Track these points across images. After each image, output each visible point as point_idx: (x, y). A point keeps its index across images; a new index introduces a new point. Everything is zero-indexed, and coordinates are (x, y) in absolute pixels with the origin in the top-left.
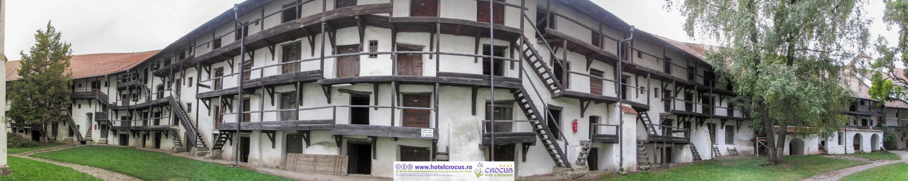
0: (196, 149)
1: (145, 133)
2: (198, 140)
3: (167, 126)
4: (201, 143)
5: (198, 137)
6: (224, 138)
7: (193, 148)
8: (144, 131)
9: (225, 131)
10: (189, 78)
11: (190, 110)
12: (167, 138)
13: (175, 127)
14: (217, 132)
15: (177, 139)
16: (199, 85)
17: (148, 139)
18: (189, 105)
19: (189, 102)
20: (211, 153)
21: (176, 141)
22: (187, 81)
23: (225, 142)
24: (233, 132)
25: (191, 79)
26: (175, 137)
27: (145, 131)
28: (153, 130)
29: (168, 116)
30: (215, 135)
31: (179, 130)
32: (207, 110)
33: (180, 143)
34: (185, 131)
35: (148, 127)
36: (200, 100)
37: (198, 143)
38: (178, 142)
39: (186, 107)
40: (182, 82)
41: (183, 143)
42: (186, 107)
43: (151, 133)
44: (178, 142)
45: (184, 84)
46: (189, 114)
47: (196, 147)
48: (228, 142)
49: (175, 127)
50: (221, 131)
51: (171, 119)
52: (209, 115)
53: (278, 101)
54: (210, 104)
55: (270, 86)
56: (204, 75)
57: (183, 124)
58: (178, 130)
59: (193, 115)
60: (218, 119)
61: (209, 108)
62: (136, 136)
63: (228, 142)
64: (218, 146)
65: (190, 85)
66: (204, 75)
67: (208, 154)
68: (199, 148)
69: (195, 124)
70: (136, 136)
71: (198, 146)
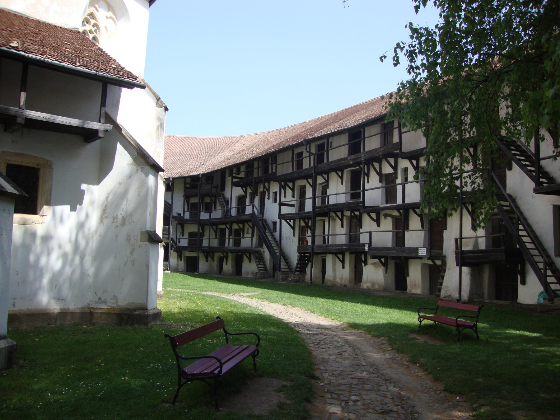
0: (279, 273)
1: (222, 255)
2: (282, 264)
3: (249, 247)
4: (286, 267)
5: (282, 257)
6: (306, 260)
7: (277, 272)
8: (221, 253)
9: (304, 253)
10: (273, 192)
12: (250, 261)
13: (261, 249)
15: (262, 263)
16: (281, 204)
17: (226, 264)
18: (275, 223)
20: (292, 278)
21: (259, 266)
22: (271, 195)
26: (259, 260)
27: (222, 253)
28: (232, 252)
29: (250, 235)
31: (264, 252)
32: (292, 231)
35: (227, 248)
36: (283, 221)
37: (282, 267)
38: (263, 266)
40: (267, 197)
41: (268, 267)
43: (230, 255)
44: (263, 266)
45: (269, 198)
46: (274, 233)
47: (280, 271)
48: (310, 264)
49: (261, 249)
51: (254, 239)
52: (294, 236)
53: (346, 221)
56: (289, 192)
58: (262, 252)
59: (277, 234)
60: (302, 240)
61: (293, 228)
62: (210, 259)
65: (275, 201)
66: (289, 192)
67: (290, 277)
68: (283, 271)
70: (210, 259)
71: (283, 270)
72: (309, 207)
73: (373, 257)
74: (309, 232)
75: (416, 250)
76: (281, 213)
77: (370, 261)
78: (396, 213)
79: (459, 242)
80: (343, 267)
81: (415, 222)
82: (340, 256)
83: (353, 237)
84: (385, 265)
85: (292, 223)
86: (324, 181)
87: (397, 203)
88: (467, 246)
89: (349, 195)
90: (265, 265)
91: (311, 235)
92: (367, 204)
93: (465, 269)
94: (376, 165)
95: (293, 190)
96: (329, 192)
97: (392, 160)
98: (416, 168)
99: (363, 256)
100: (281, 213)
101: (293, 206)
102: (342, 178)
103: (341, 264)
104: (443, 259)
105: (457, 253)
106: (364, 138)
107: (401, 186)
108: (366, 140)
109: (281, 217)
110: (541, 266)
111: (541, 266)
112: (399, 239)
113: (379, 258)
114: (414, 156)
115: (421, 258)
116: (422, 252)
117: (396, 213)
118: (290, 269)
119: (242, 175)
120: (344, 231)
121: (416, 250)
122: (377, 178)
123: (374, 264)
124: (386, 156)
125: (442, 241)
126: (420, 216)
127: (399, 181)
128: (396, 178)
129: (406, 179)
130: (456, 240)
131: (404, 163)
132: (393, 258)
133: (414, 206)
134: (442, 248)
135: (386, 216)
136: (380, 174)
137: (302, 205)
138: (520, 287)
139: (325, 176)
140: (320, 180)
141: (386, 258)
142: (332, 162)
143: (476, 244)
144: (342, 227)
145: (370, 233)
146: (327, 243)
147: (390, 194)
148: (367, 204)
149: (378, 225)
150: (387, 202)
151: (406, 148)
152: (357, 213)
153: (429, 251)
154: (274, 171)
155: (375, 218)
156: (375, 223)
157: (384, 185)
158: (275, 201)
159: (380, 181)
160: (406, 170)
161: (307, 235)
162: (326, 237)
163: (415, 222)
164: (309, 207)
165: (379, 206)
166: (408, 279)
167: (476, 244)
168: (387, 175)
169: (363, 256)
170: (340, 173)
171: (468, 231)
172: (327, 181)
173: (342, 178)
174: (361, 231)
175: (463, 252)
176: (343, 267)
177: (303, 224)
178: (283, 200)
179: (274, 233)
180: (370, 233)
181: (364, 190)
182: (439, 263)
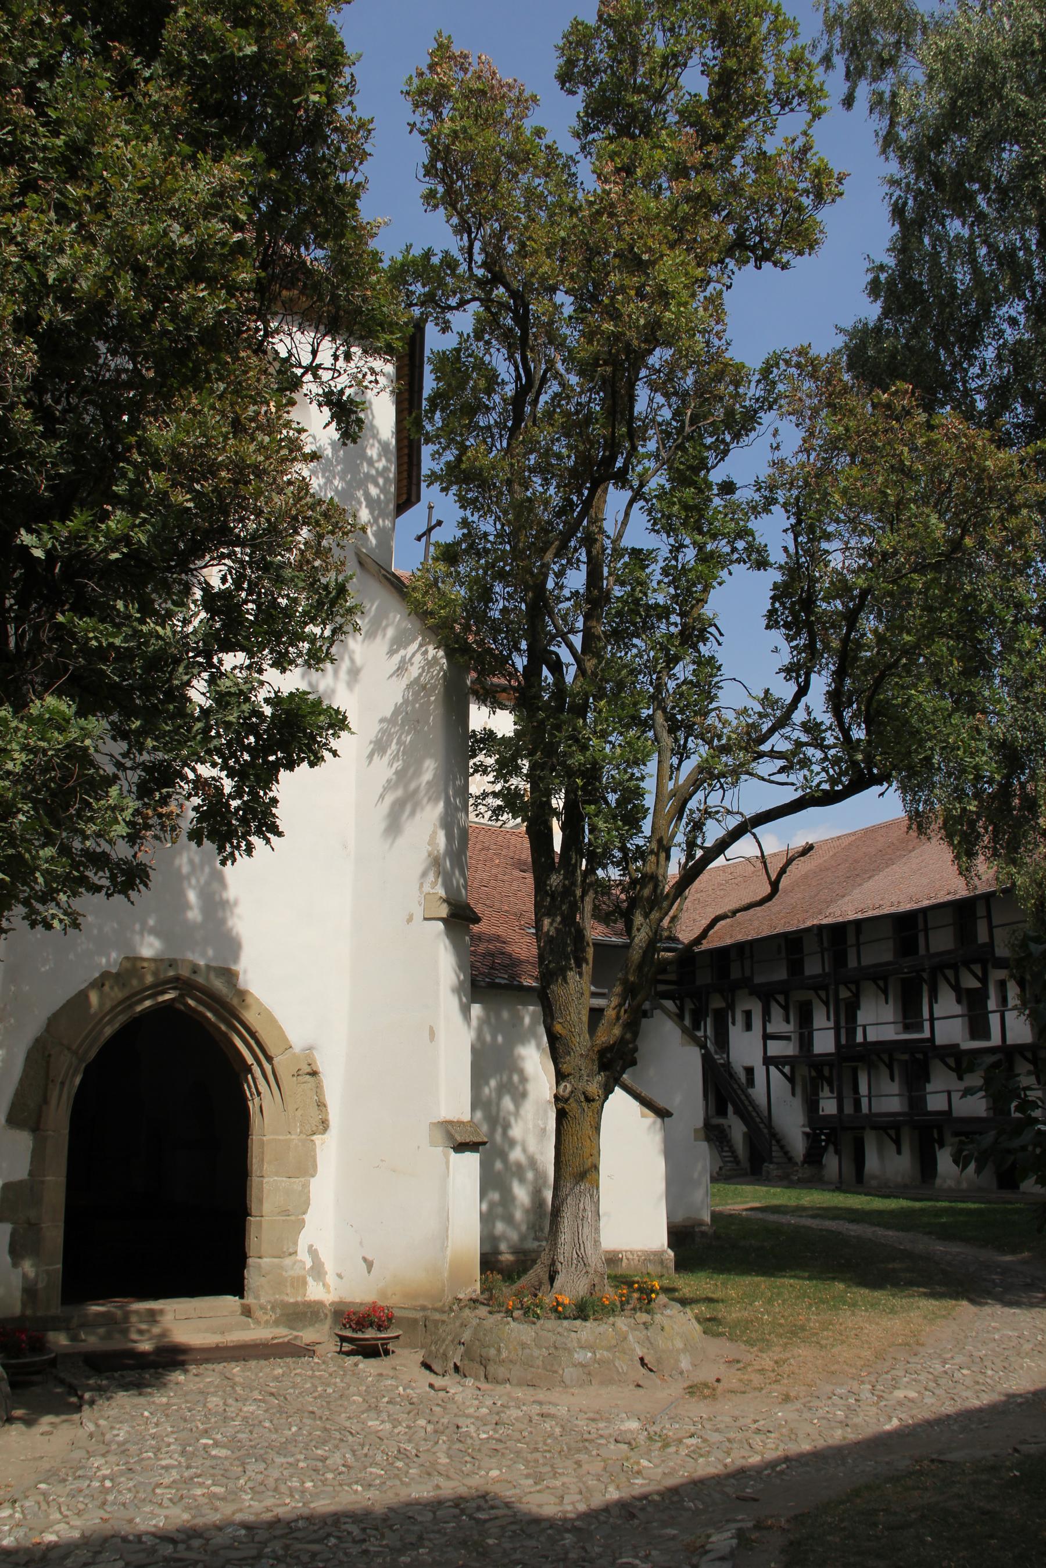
9: (821, 1129)
11: (751, 1082)
14: (808, 1130)
16: (766, 1037)
18: (750, 1071)
19: (748, 1064)
22: (739, 1018)
23: (825, 1148)
25: (748, 1015)
32: (788, 1085)
34: (745, 1129)
36: (772, 1068)
39: (742, 1077)
42: (742, 1077)
45: (734, 1024)
46: (750, 1091)
48: (831, 1149)
52: (793, 1094)
54: (792, 1070)
56: (777, 1012)
57: (738, 1112)
59: (758, 1092)
60: (811, 1106)
61: (791, 1079)
63: (831, 1149)
64: (814, 1156)
65: (748, 1027)
66: (777, 1012)
69: (766, 1113)
72: (824, 1043)
74: (826, 1088)
76: (769, 1054)
80: (899, 1152)
82: (892, 1132)
83: (916, 1101)
85: (787, 1069)
86: (849, 994)
89: (900, 1026)
90: (733, 1151)
91: (830, 1095)
94: (949, 973)
95: (786, 1008)
96: (862, 1017)
97: (978, 969)
99: (935, 1132)
100: (769, 1054)
103: (894, 1147)
106: (926, 930)
107: (998, 1015)
108: (931, 934)
109: (768, 1061)
119: (673, 977)
120: (895, 1088)
122: (952, 996)
124: (967, 964)
127: (992, 1004)
128: (987, 997)
129: (1004, 1000)
136: (957, 988)
137: (806, 1041)
139: (853, 987)
140: (844, 994)
145: (949, 1093)
146: (865, 1109)
147: (978, 1027)
149: (960, 1078)
152: (920, 1056)
154: (748, 973)
155: (953, 1065)
156: (954, 1075)
157: (966, 1012)
158: (748, 1027)
159: (959, 1001)
161: (821, 1095)
162: (865, 1101)
164: (824, 1043)
165: (958, 1045)
168: (969, 991)
169: (935, 1132)
170: (881, 983)
172: (857, 996)
173: (885, 993)
174: (929, 1088)
176: (899, 1152)
177: (814, 1074)
178: (770, 1029)
179: (750, 1091)
180: (949, 1093)
181: (932, 1019)
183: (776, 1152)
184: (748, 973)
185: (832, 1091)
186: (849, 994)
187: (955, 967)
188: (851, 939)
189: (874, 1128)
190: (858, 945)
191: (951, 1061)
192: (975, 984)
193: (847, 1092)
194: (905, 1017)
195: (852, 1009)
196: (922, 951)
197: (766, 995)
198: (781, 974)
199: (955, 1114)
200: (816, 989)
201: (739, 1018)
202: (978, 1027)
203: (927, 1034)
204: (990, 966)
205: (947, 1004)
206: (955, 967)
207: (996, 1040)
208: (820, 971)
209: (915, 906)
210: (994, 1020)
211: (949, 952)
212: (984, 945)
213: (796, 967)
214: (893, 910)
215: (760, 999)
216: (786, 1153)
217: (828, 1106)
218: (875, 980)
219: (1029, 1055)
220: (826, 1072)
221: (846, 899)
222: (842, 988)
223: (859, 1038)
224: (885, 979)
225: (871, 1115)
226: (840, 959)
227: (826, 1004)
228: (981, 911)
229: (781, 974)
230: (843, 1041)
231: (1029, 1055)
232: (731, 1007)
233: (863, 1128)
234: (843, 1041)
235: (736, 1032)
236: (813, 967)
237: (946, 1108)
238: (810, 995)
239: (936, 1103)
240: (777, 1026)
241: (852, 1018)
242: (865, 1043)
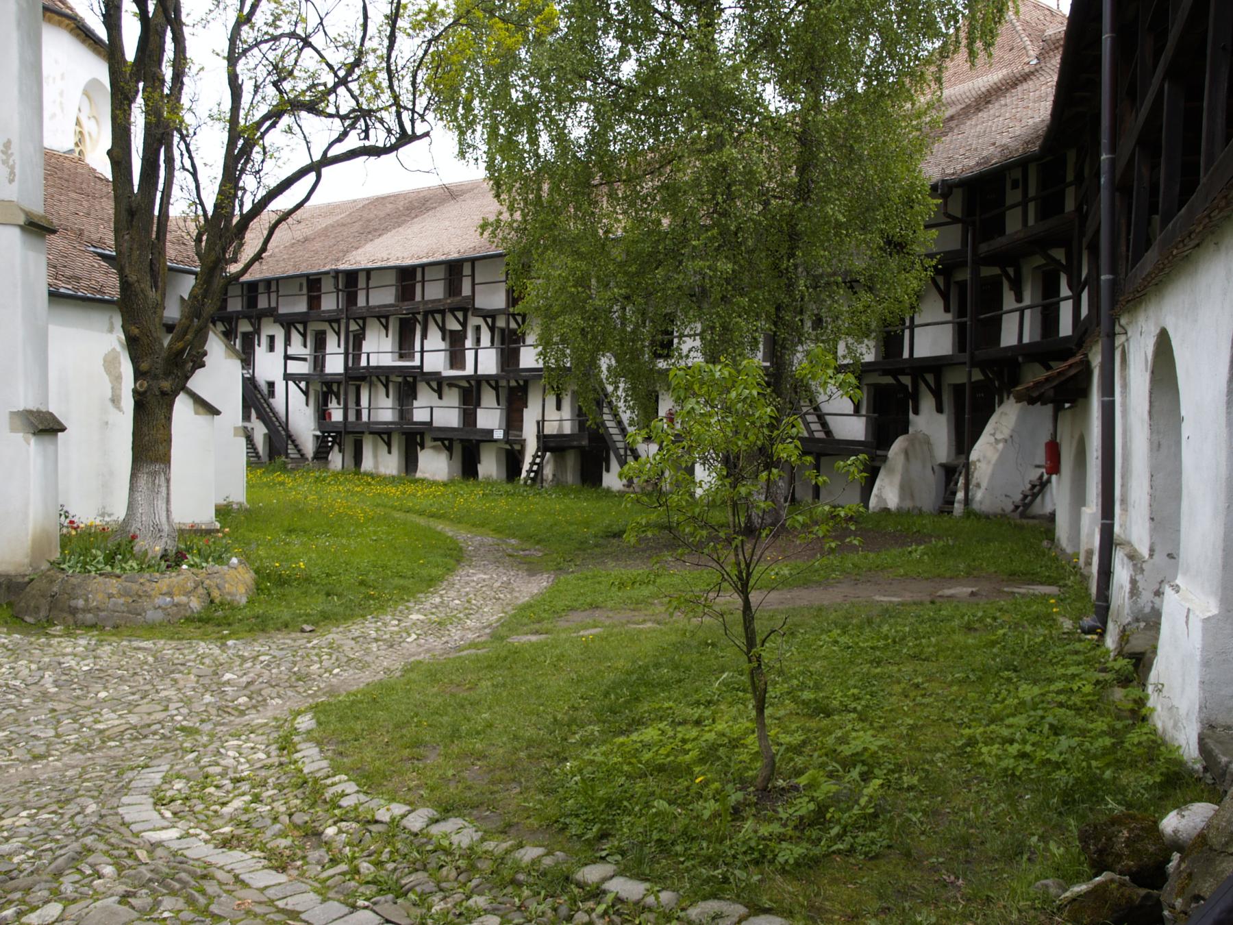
11: (272, 393)
14: (318, 433)
16: (287, 357)
18: (271, 385)
19: (271, 379)
22: (264, 341)
23: (331, 448)
24: (339, 433)
25: (272, 339)
30: (317, 437)
32: (303, 397)
33: (257, 453)
36: (290, 383)
46: (271, 400)
48: (336, 448)
50: (323, 432)
55: (381, 376)
56: (296, 338)
57: (260, 417)
59: (278, 402)
60: (322, 415)
61: (306, 393)
63: (336, 448)
64: (322, 454)
65: (271, 348)
66: (296, 338)
69: (284, 419)
72: (335, 364)
73: (435, 440)
74: (334, 401)
75: (491, 432)
76: (289, 371)
77: (428, 442)
78: (465, 384)
79: (540, 424)
80: (390, 452)
81: (488, 398)
82: (385, 437)
84: (449, 449)
85: (303, 385)
86: (357, 328)
87: (463, 367)
88: (551, 429)
92: (426, 369)
93: (548, 454)
94: (438, 317)
95: (304, 335)
96: (366, 346)
97: (460, 315)
98: (492, 329)
100: (289, 371)
101: (305, 360)
102: (386, 328)
103: (386, 448)
104: (522, 443)
105: (538, 437)
106: (423, 282)
109: (287, 377)
110: (622, 452)
111: (622, 452)
112: (469, 417)
113: (442, 440)
114: (490, 316)
115: (496, 441)
116: (498, 434)
117: (466, 385)
118: (302, 455)
121: (491, 432)
122: (439, 334)
123: (434, 448)
124: (453, 311)
125: (522, 421)
126: (496, 388)
127: (469, 343)
128: (465, 338)
129: (478, 341)
130: (538, 423)
131: (474, 321)
132: (462, 441)
133: (487, 379)
134: (521, 429)
135: (451, 385)
136: (443, 329)
137: (319, 362)
138: (604, 473)
139: (361, 322)
140: (353, 327)
141: (451, 441)
142: (375, 307)
143: (561, 427)
144: (387, 396)
146: (365, 418)
147: (456, 358)
148: (426, 369)
149: (440, 397)
150: (452, 367)
151: (482, 302)
153: (506, 433)
155: (435, 387)
156: (436, 395)
158: (271, 348)
159: (444, 339)
160: (478, 328)
163: (488, 398)
165: (439, 373)
166: (479, 467)
167: (561, 427)
168: (451, 332)
170: (383, 321)
171: (551, 413)
172: (363, 329)
173: (386, 328)
174: (416, 404)
175: (545, 436)
176: (390, 452)
178: (290, 352)
179: (271, 400)
181: (422, 351)
182: (517, 447)
183: (291, 451)
184: (273, 304)
185: (339, 403)
186: (357, 328)
187: (442, 312)
188: (362, 283)
189: (371, 433)
190: (368, 289)
191: (434, 385)
192: (456, 327)
193: (351, 404)
194: (400, 348)
195: (359, 339)
196: (418, 298)
197: (288, 323)
198: (301, 307)
199: (435, 424)
200: (330, 321)
201: (264, 341)
202: (456, 358)
203: (417, 362)
204: (470, 313)
205: (435, 340)
206: (442, 312)
207: (469, 370)
208: (334, 307)
209: (417, 262)
210: (470, 356)
211: (439, 300)
212: (467, 297)
213: (314, 302)
214: (398, 263)
215: (283, 326)
216: (299, 451)
217: (337, 415)
218: (378, 318)
219: (493, 383)
220: (335, 388)
221: (360, 251)
222: (352, 322)
223: (363, 363)
224: (387, 318)
225: (369, 423)
226: (351, 299)
227: (338, 334)
228: (467, 270)
229: (301, 307)
230: (350, 364)
231: (493, 383)
232: (257, 331)
233: (363, 433)
234: (350, 364)
235: (261, 352)
236: (329, 303)
237: (428, 420)
238: (325, 326)
239: (420, 415)
240: (296, 348)
241: (358, 346)
242: (368, 367)
